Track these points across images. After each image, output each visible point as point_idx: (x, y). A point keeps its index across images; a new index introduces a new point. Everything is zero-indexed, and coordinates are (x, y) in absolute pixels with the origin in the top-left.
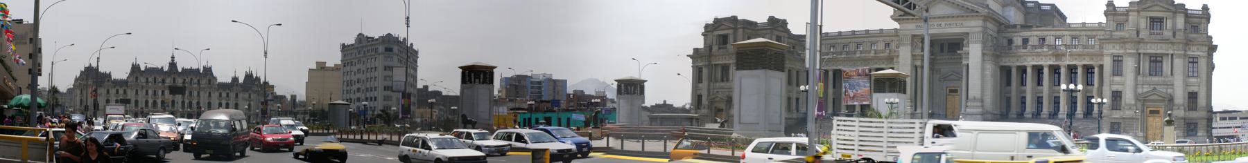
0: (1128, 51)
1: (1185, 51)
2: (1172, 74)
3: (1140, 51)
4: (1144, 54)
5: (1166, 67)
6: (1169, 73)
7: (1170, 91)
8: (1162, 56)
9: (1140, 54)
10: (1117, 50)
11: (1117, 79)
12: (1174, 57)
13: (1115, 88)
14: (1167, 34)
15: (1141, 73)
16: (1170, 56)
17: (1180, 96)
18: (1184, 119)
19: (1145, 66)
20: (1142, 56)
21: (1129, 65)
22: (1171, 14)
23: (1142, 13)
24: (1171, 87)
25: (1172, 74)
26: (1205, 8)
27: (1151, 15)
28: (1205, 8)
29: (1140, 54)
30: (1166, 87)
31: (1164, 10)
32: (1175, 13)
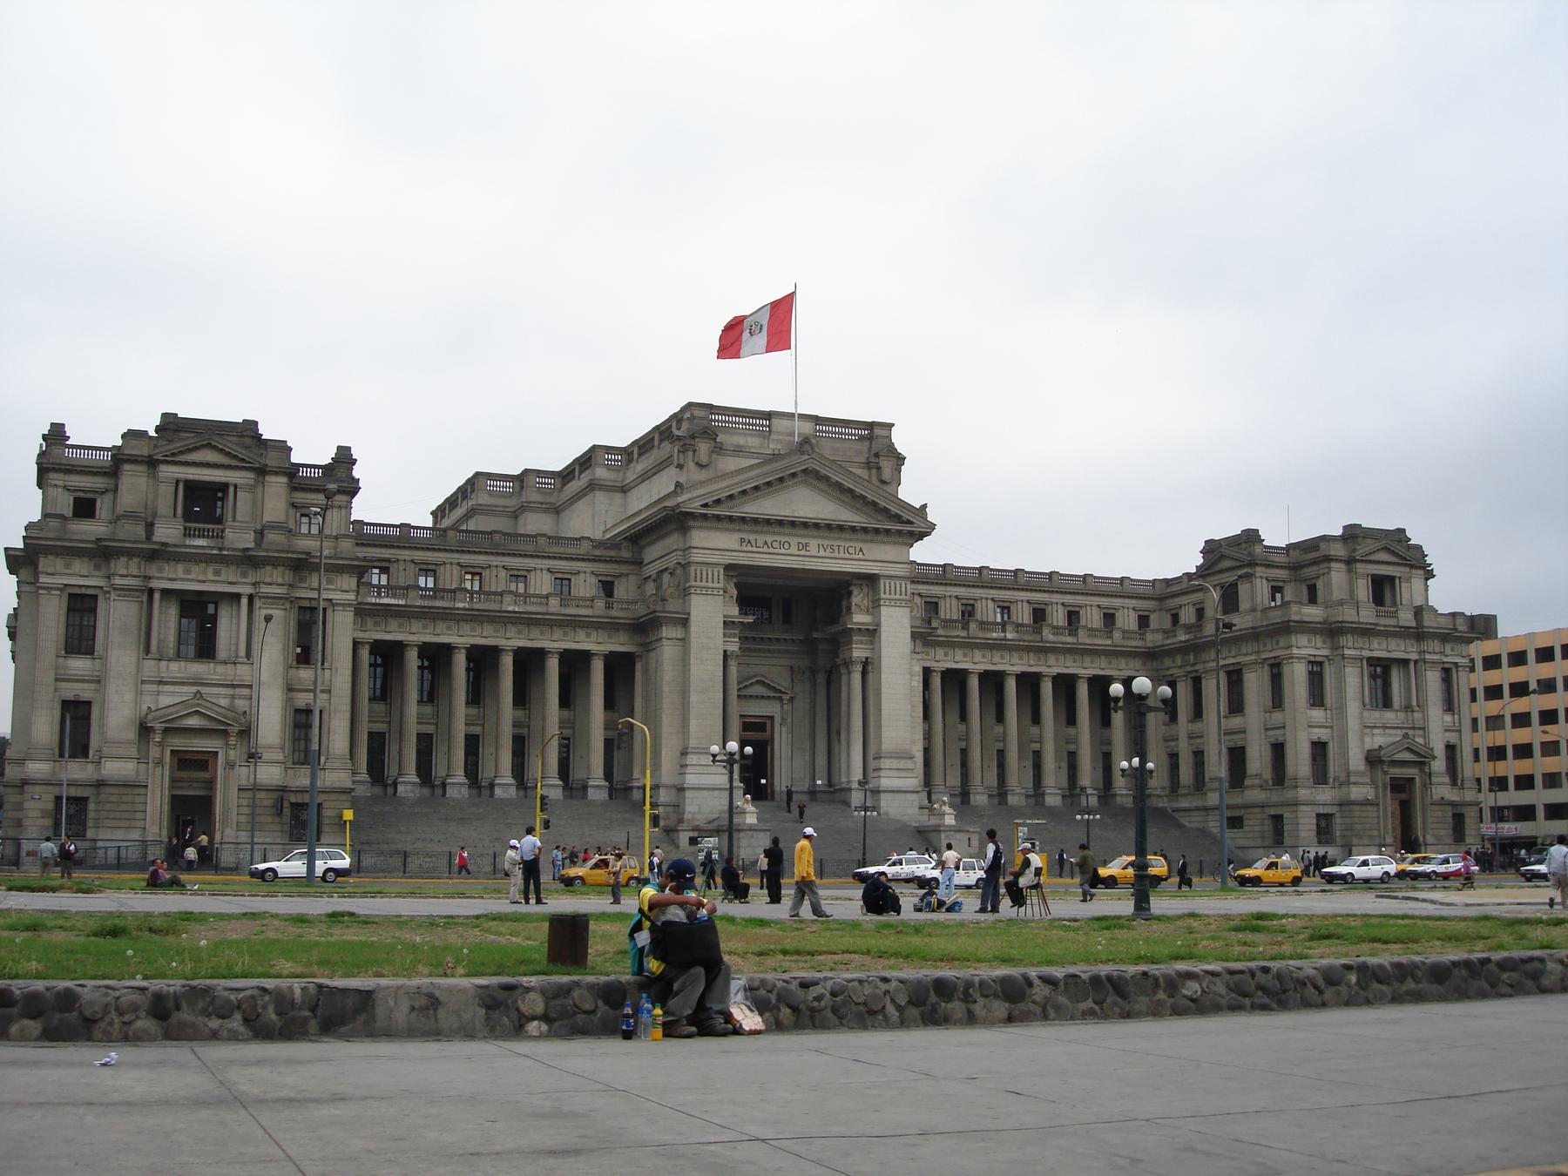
0: (118, 581)
1: (291, 586)
2: (249, 654)
3: (155, 584)
4: (166, 593)
5: (229, 628)
6: (242, 653)
7: (241, 704)
8: (218, 598)
9: (151, 591)
10: (82, 576)
11: (79, 664)
12: (257, 603)
13: (72, 691)
14: (239, 537)
15: (154, 647)
16: (244, 601)
17: (271, 724)
18: (283, 790)
19: (168, 621)
20: (157, 596)
21: (117, 617)
22: (252, 475)
23: (169, 472)
24: (246, 692)
25: (249, 654)
26: (344, 458)
27: (191, 477)
28: (344, 458)
29: (151, 591)
30: (230, 691)
31: (234, 462)
32: (262, 471)
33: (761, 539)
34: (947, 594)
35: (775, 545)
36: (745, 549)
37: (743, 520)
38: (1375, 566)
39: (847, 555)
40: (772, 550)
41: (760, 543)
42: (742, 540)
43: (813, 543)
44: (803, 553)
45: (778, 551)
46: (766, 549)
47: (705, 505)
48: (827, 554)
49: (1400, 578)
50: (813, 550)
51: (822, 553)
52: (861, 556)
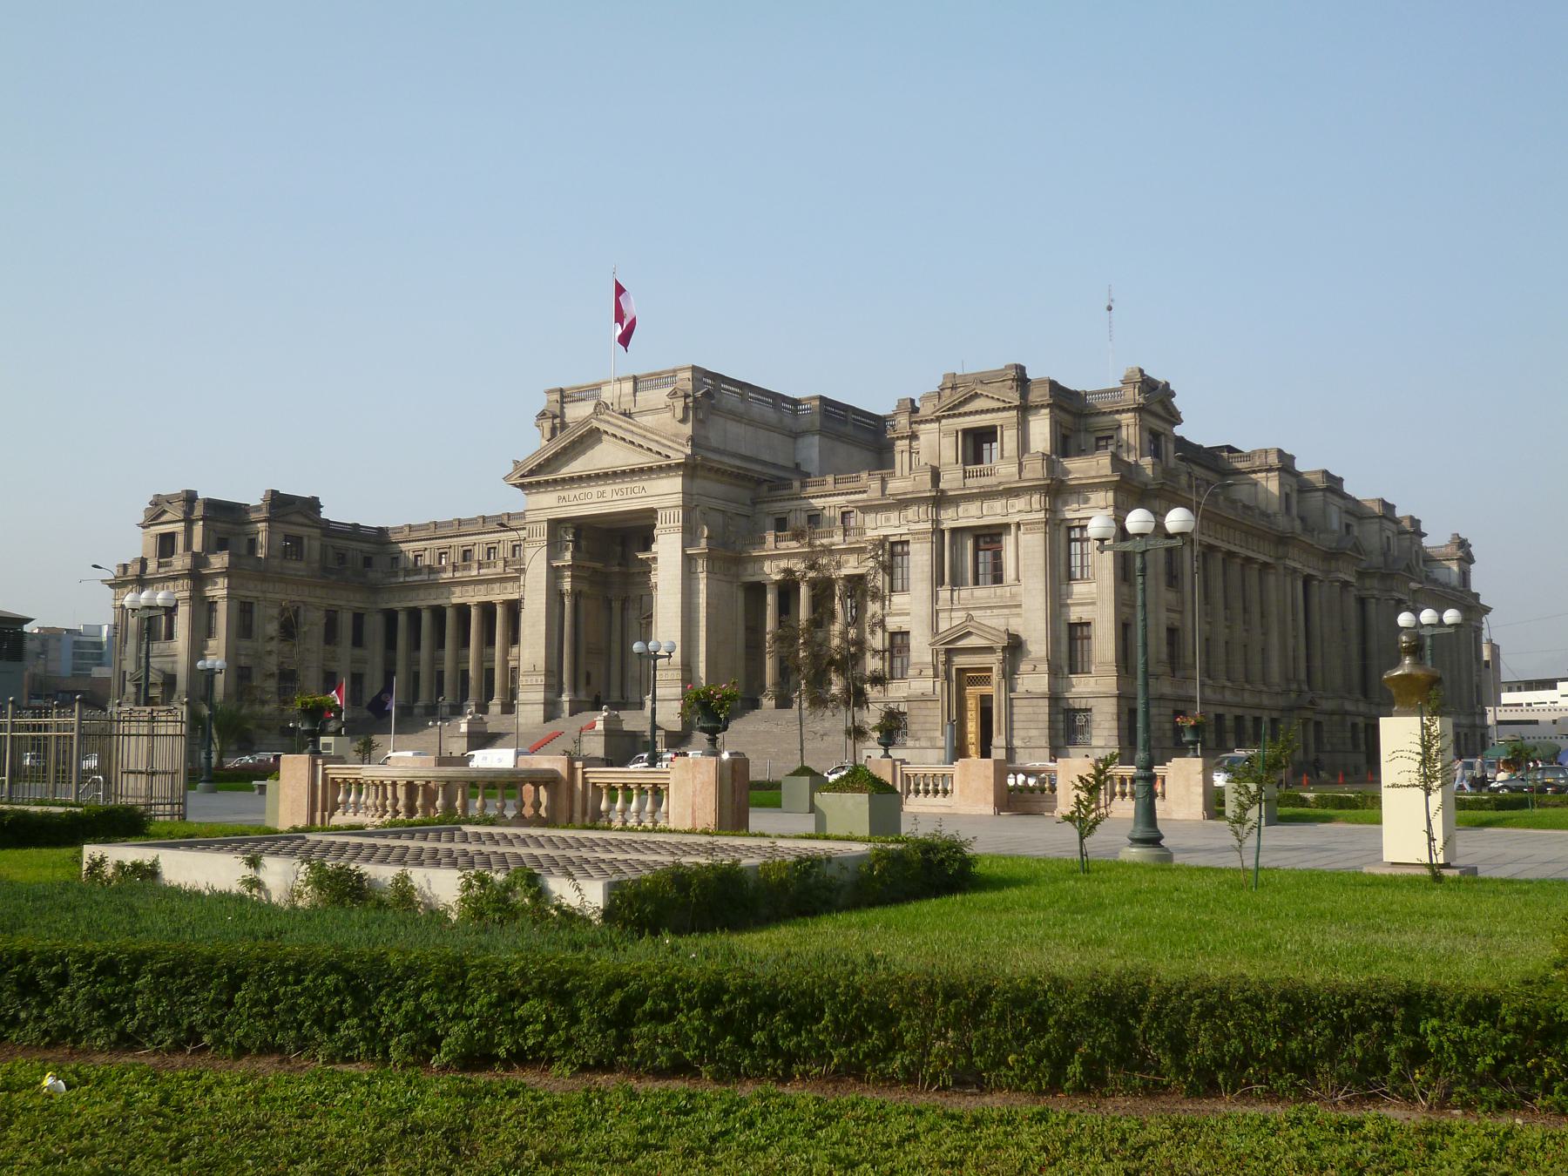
33: (572, 493)
34: (826, 505)
35: (582, 497)
36: (561, 504)
37: (563, 480)
38: (967, 419)
39: (633, 495)
40: (580, 502)
41: (595, 496)
42: (559, 499)
43: (608, 489)
44: (600, 500)
45: (584, 502)
46: (575, 502)
47: (523, 476)
48: (619, 497)
49: (1002, 426)
50: (608, 496)
51: (615, 497)
52: (643, 494)
